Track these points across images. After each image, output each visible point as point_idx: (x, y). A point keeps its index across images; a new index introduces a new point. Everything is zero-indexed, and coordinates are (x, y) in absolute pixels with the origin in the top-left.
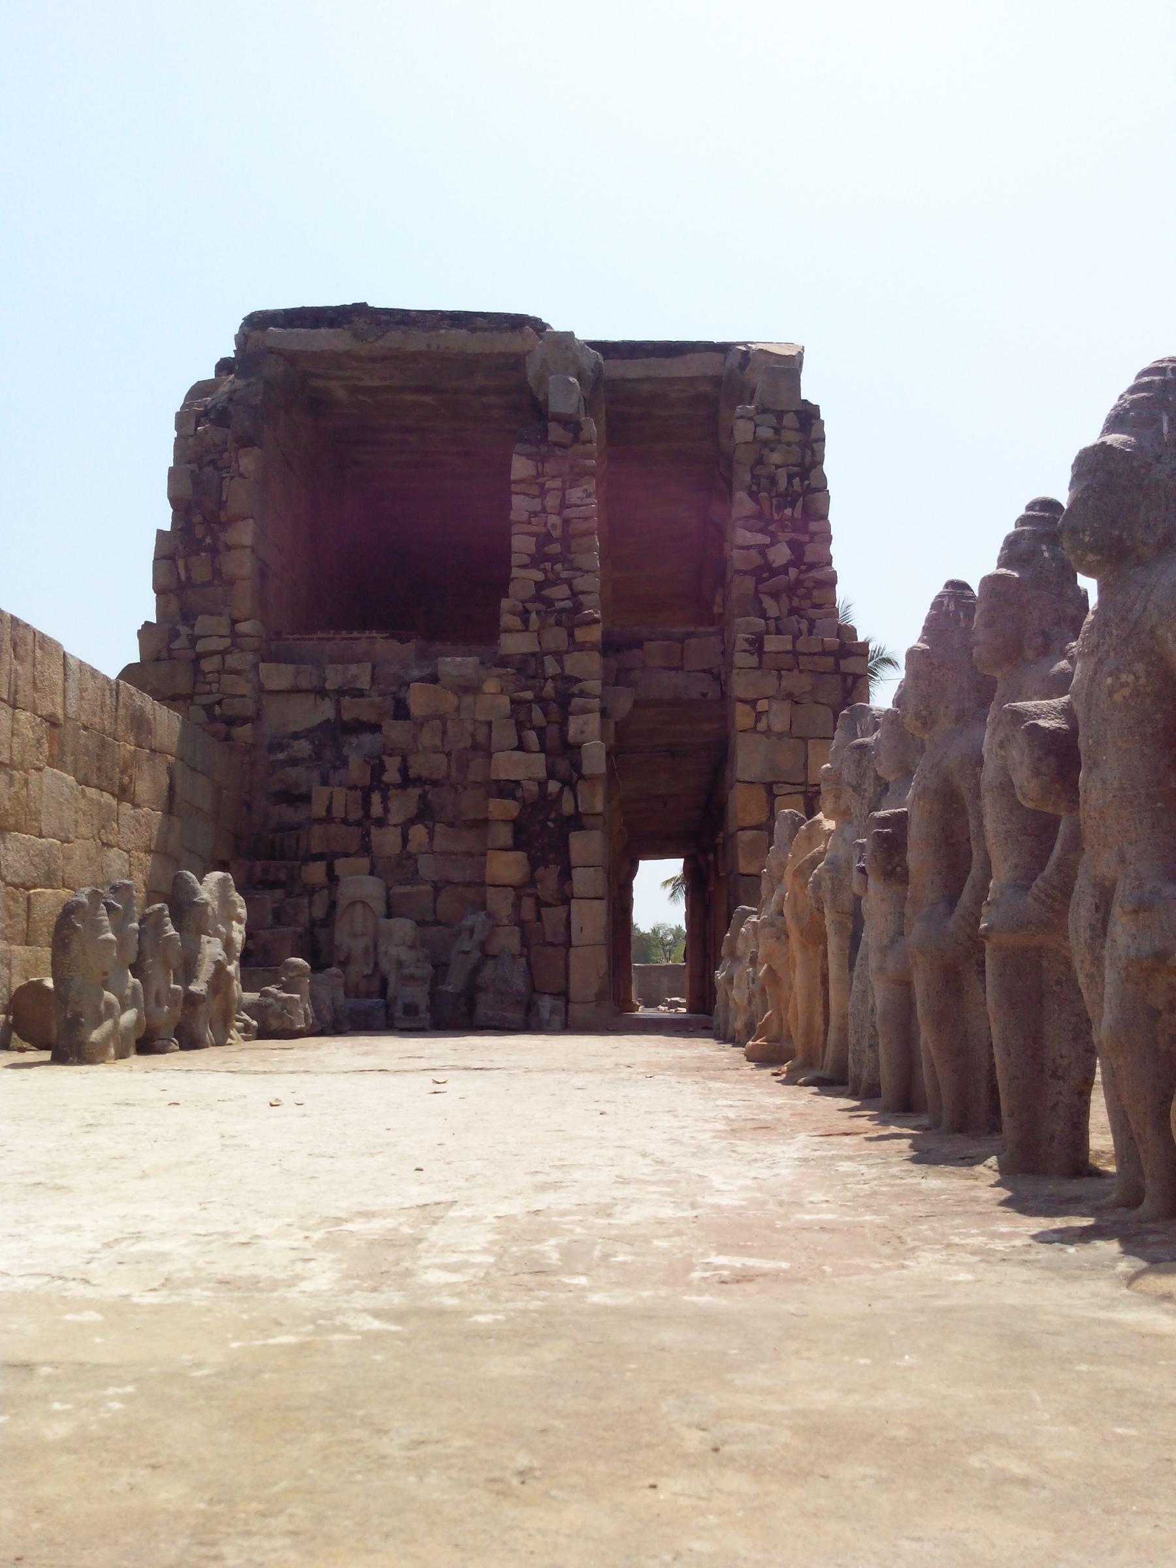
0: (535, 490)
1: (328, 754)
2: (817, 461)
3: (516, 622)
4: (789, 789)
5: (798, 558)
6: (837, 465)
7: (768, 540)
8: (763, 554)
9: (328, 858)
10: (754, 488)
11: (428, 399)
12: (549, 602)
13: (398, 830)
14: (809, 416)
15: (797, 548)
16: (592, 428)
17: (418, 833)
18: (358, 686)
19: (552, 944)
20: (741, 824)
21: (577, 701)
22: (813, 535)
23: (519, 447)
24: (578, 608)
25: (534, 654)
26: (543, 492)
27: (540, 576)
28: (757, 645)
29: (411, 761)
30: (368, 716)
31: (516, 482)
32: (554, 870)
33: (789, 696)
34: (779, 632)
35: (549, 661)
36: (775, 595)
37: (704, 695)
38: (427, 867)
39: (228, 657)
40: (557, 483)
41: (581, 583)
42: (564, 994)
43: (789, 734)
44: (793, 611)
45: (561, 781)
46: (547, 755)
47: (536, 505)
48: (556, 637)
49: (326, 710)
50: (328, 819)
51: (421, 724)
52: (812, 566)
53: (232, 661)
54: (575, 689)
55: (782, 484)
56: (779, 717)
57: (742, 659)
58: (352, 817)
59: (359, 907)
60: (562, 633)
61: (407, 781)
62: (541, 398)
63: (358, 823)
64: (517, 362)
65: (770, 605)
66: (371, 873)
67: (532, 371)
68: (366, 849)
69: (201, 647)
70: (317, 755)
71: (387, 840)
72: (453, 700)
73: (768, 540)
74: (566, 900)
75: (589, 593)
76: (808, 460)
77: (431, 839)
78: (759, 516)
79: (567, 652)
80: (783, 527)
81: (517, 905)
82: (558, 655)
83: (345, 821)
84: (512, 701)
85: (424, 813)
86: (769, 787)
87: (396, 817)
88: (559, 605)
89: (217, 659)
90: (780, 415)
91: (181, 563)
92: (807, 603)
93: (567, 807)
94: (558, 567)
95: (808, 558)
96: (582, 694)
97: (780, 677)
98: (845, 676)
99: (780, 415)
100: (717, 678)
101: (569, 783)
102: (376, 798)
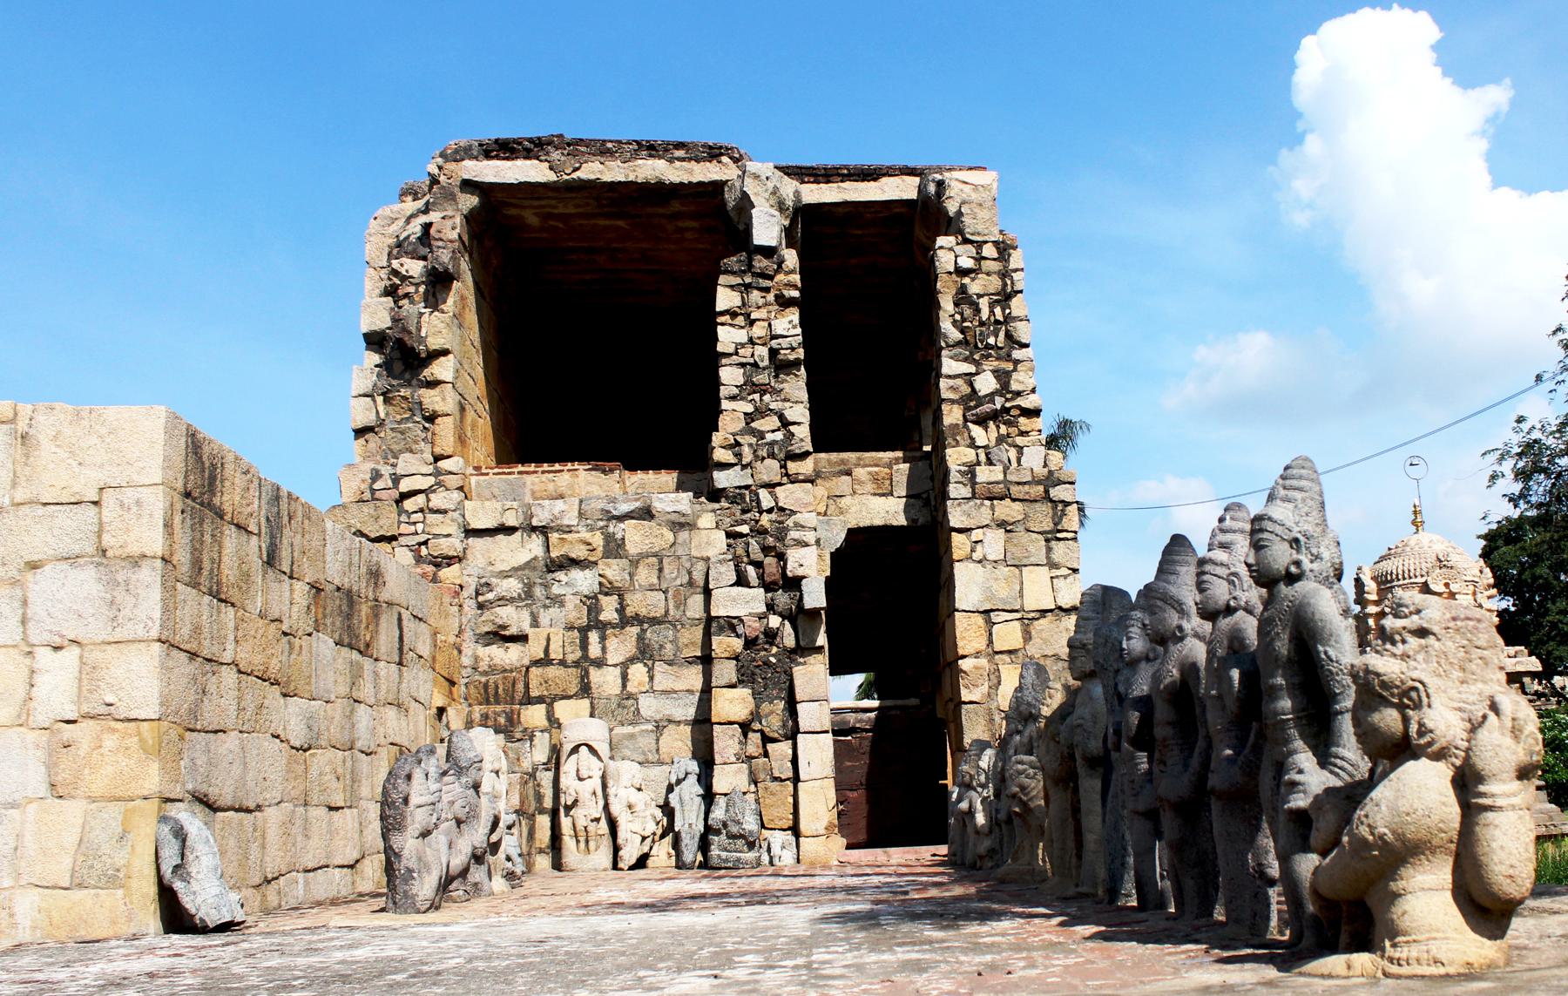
1: (538, 592)
7: (972, 369)
8: (971, 385)
9: (548, 701)
11: (620, 223)
12: (761, 435)
13: (618, 671)
15: (1003, 377)
17: (638, 672)
18: (566, 522)
25: (747, 487)
27: (750, 408)
28: (970, 472)
29: (628, 598)
30: (579, 552)
31: (722, 313)
33: (1002, 524)
34: (990, 462)
35: (764, 494)
36: (982, 421)
38: (649, 706)
39: (432, 496)
40: (762, 314)
41: (790, 415)
42: (795, 830)
44: (1001, 440)
45: (780, 615)
47: (741, 336)
48: (769, 470)
49: (533, 547)
50: (545, 661)
51: (635, 563)
53: (437, 500)
54: (790, 522)
56: (994, 544)
57: (956, 490)
58: (570, 658)
59: (583, 749)
60: (774, 464)
61: (625, 621)
62: (741, 227)
63: (576, 664)
65: (977, 431)
66: (592, 715)
68: (585, 690)
69: (405, 486)
70: (528, 594)
71: (606, 681)
72: (670, 536)
73: (972, 369)
74: (793, 734)
75: (799, 424)
77: (651, 678)
78: (964, 343)
79: (780, 484)
80: (987, 357)
82: (770, 486)
83: (563, 663)
84: (729, 535)
85: (645, 653)
87: (614, 657)
88: (769, 437)
89: (421, 499)
90: (979, 245)
91: (380, 399)
94: (767, 398)
95: (1014, 386)
96: (798, 526)
97: (992, 508)
99: (979, 245)
102: (594, 637)
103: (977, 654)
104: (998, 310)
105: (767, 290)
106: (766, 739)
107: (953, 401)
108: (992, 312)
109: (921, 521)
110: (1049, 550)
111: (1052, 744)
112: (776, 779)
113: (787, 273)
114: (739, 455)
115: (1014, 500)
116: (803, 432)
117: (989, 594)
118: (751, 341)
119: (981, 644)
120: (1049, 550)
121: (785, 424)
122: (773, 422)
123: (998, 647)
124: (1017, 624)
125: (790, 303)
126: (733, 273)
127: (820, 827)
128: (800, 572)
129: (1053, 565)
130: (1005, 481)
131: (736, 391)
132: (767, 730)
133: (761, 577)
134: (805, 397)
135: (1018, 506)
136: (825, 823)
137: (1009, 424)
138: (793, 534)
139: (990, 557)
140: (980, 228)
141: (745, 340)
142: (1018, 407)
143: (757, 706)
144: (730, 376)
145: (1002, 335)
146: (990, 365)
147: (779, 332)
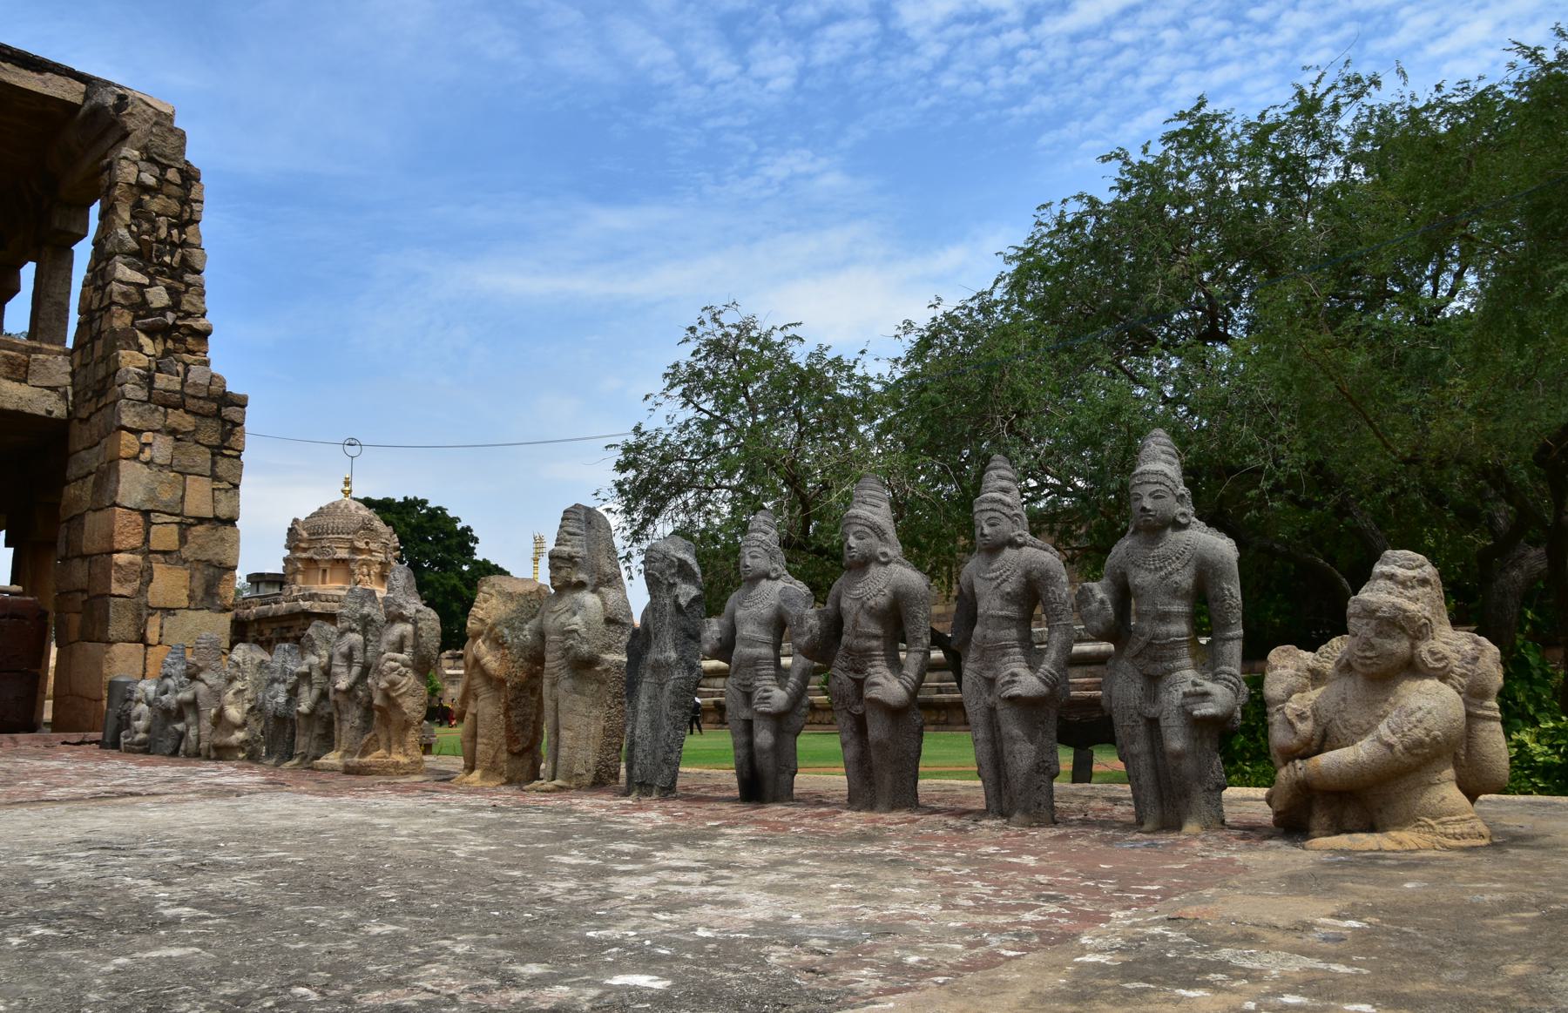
6: (216, 230)
7: (146, 281)
8: (143, 295)
10: (134, 228)
14: (190, 177)
20: (117, 546)
22: (188, 285)
33: (173, 432)
34: (159, 370)
36: (151, 332)
37: (50, 412)
52: (189, 315)
55: (163, 233)
56: (162, 448)
57: (132, 390)
65: (143, 339)
73: (146, 281)
76: (186, 216)
80: (162, 273)
90: (164, 168)
95: (186, 307)
97: (166, 415)
98: (224, 421)
100: (64, 396)
103: (133, 551)
104: (175, 232)
107: (123, 306)
108: (169, 234)
109: (56, 413)
110: (214, 463)
115: (187, 412)
117: (152, 494)
119: (136, 541)
120: (214, 463)
123: (154, 545)
124: (175, 528)
129: (215, 477)
130: (181, 392)
135: (189, 418)
137: (175, 340)
140: (168, 151)
142: (190, 327)
145: (177, 257)
146: (163, 281)
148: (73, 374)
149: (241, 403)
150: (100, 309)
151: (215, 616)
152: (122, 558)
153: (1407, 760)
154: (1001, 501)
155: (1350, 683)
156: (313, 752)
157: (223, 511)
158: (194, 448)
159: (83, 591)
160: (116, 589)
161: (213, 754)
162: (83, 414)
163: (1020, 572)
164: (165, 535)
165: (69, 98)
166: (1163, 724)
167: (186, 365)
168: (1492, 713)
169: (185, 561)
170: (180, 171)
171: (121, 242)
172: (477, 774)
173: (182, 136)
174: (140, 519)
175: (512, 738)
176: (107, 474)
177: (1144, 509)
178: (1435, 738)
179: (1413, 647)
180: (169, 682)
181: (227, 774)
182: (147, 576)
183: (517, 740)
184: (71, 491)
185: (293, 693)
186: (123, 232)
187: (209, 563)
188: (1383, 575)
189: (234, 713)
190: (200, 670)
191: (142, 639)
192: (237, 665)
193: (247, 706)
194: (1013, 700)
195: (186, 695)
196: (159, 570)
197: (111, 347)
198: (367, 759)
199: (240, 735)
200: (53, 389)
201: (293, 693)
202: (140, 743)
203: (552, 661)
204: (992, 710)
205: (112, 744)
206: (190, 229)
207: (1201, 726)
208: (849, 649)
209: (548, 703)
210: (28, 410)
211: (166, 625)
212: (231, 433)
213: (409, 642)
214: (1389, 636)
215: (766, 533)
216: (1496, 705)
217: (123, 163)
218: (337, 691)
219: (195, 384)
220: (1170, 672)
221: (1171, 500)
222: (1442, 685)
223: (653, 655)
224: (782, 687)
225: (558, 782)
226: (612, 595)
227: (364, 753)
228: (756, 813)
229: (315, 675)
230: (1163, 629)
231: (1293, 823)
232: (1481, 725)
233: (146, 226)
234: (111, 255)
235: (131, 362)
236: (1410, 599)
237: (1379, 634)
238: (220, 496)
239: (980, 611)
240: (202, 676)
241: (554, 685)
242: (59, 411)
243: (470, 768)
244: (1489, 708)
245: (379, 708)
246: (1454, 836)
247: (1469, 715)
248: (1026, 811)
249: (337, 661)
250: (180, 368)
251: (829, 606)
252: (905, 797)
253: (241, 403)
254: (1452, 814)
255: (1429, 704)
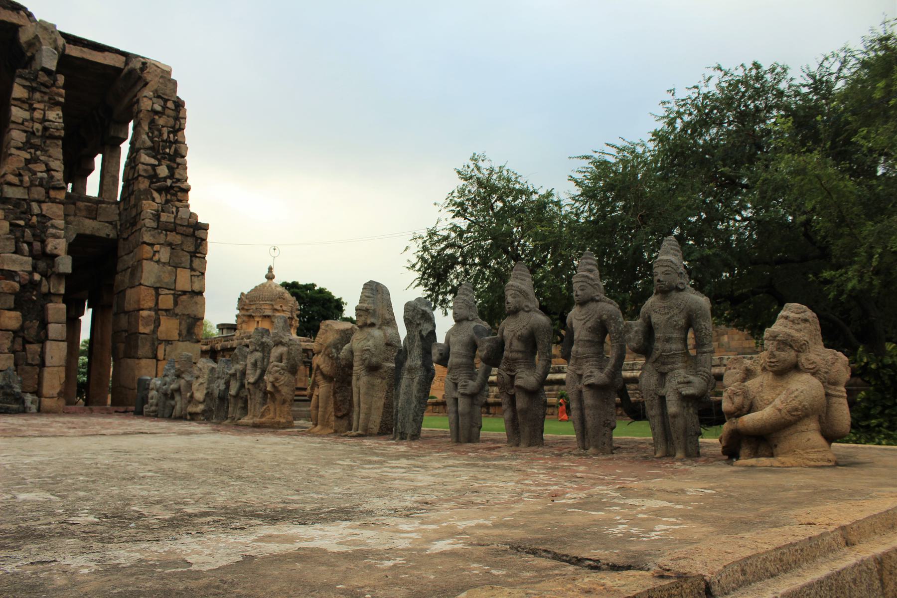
0: (26, 106)
2: (181, 129)
3: (15, 180)
4: (167, 292)
5: (171, 176)
6: (192, 134)
7: (157, 163)
8: (154, 170)
10: (150, 134)
12: (34, 173)
14: (179, 105)
16: (61, 79)
19: (31, 365)
20: (142, 307)
21: (51, 231)
22: (179, 164)
23: (18, 80)
24: (51, 177)
25: (24, 200)
26: (32, 109)
27: (28, 156)
31: (15, 99)
32: (36, 323)
33: (170, 245)
34: (163, 211)
35: (34, 205)
36: (159, 191)
37: (108, 235)
40: (41, 106)
42: (38, 393)
43: (169, 264)
44: (167, 202)
46: (33, 259)
47: (26, 115)
52: (178, 180)
54: (49, 224)
56: (164, 254)
60: (42, 190)
64: (14, 29)
65: (156, 195)
67: (24, 37)
73: (157, 163)
76: (177, 127)
78: (151, 148)
79: (44, 202)
80: (164, 158)
81: (13, 342)
84: (11, 225)
86: (157, 289)
88: (39, 175)
90: (166, 101)
92: (174, 198)
93: (44, 289)
94: (38, 153)
95: (177, 176)
96: (53, 226)
97: (166, 235)
98: (197, 238)
100: (115, 226)
101: (44, 275)
103: (150, 309)
104: (171, 136)
105: (45, 93)
106: (26, 342)
107: (145, 177)
108: (169, 137)
109: (111, 236)
110: (191, 261)
111: (327, 358)
112: (28, 364)
113: (59, 87)
114: (21, 181)
115: (177, 233)
116: (59, 176)
118: (32, 119)
119: (151, 304)
120: (191, 261)
121: (49, 170)
122: (43, 167)
123: (161, 306)
124: (172, 297)
125: (58, 104)
126: (26, 79)
127: (55, 392)
128: (55, 252)
130: (175, 223)
131: (21, 145)
132: (26, 336)
133: (31, 251)
134: (61, 158)
135: (179, 237)
136: (58, 390)
137: (173, 195)
138: (51, 231)
139: (163, 260)
140: (168, 92)
141: (28, 117)
142: (179, 187)
143: (23, 323)
144: (17, 136)
146: (165, 163)
147: (51, 118)
148: (120, 214)
149: (205, 227)
150: (133, 179)
151: (193, 345)
152: (144, 313)
153: (789, 418)
154: (587, 277)
155: (766, 377)
156: (238, 416)
157: (196, 288)
158: (181, 253)
159: (126, 331)
160: (142, 329)
161: (188, 417)
162: (125, 236)
163: (596, 316)
164: (167, 301)
165: (117, 65)
166: (667, 399)
167: (177, 208)
168: (840, 394)
169: (177, 315)
170: (174, 102)
171: (144, 142)
172: (319, 427)
173: (175, 83)
174: (154, 292)
175: (337, 409)
176: (136, 269)
177: (659, 281)
178: (804, 406)
179: (797, 356)
180: (168, 379)
181: (193, 426)
182: (157, 323)
183: (340, 410)
184: (119, 277)
185: (227, 384)
186: (145, 137)
187: (189, 316)
188: (782, 317)
189: (199, 395)
190: (183, 372)
191: (155, 357)
192: (200, 369)
193: (205, 392)
194: (590, 386)
195: (174, 386)
196: (163, 320)
197: (139, 200)
198: (263, 420)
199: (201, 407)
200: (110, 223)
201: (227, 384)
202: (153, 412)
203: (357, 367)
204: (580, 392)
205: (139, 413)
206: (179, 133)
207: (686, 399)
208: (507, 358)
209: (355, 389)
210: (97, 234)
211: (168, 349)
212: (201, 244)
213: (284, 357)
214: (783, 351)
215: (467, 295)
216: (843, 389)
217: (145, 99)
218: (249, 383)
219: (182, 218)
220: (672, 370)
221: (674, 275)
222: (812, 377)
223: (408, 363)
224: (472, 380)
225: (360, 432)
226: (389, 331)
227: (263, 416)
228: (455, 448)
229: (238, 374)
230: (668, 346)
231: (731, 452)
232: (834, 399)
233: (156, 133)
234: (139, 149)
235: (149, 207)
236: (797, 330)
237: (778, 349)
238: (195, 279)
239: (575, 337)
240: (184, 376)
241: (358, 379)
242: (113, 234)
243: (316, 425)
244: (839, 391)
245: (270, 392)
246: (812, 460)
247: (827, 395)
248: (596, 447)
249: (249, 366)
250: (174, 210)
251: (498, 335)
252: (536, 439)
253: (205, 227)
254: (813, 448)
255: (804, 388)
